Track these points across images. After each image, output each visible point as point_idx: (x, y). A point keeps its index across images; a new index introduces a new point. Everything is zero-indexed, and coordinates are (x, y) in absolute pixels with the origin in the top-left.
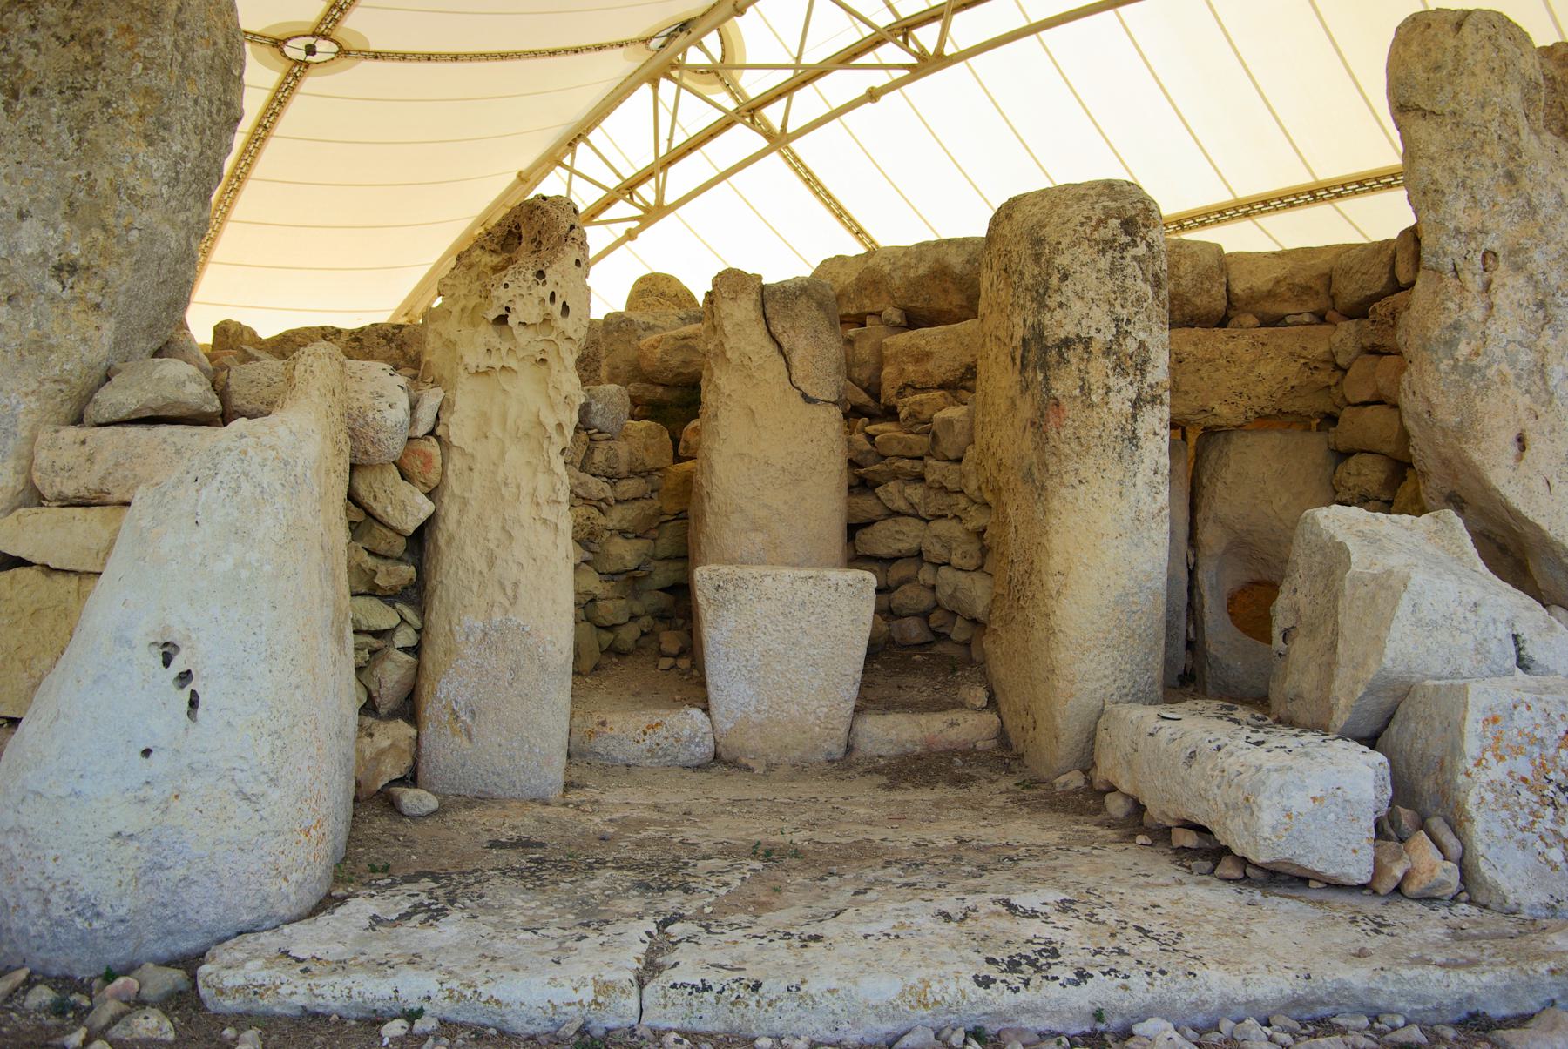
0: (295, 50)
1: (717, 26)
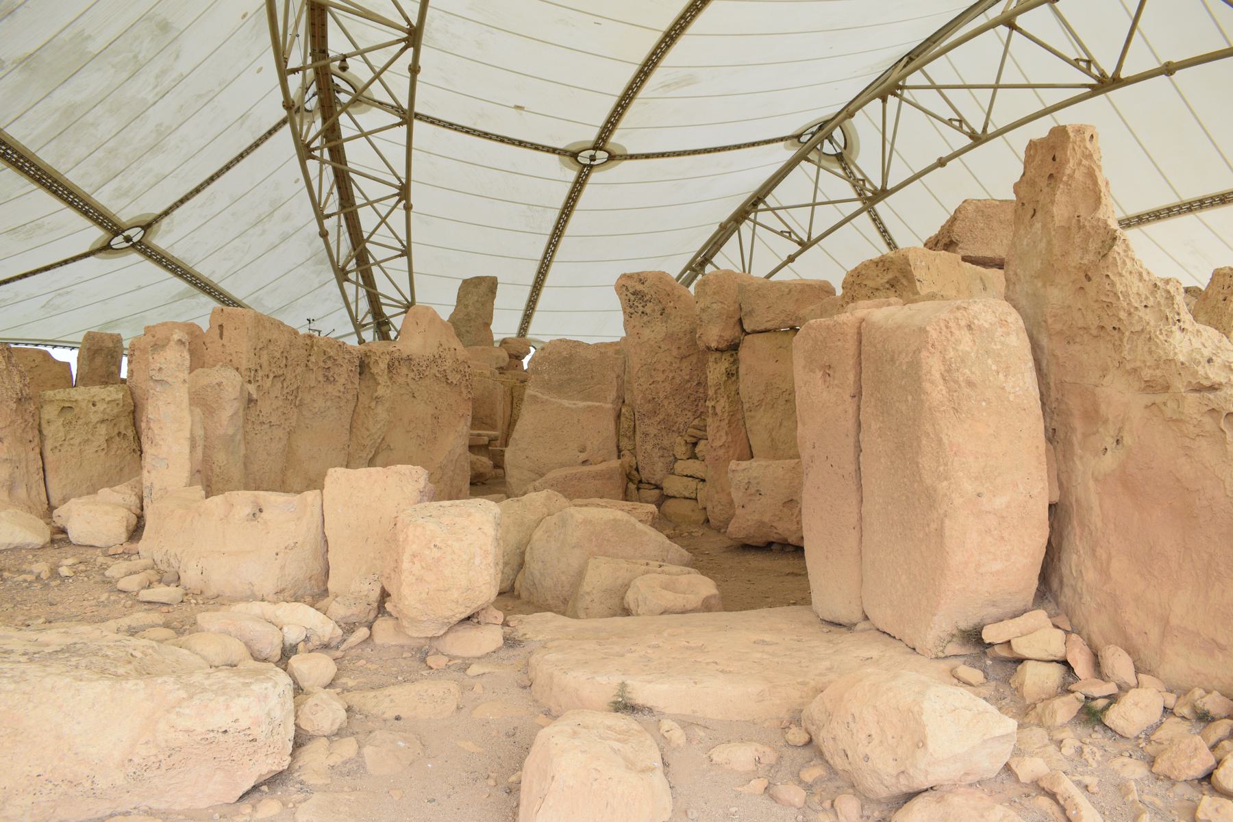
0: (584, 158)
1: (839, 124)
